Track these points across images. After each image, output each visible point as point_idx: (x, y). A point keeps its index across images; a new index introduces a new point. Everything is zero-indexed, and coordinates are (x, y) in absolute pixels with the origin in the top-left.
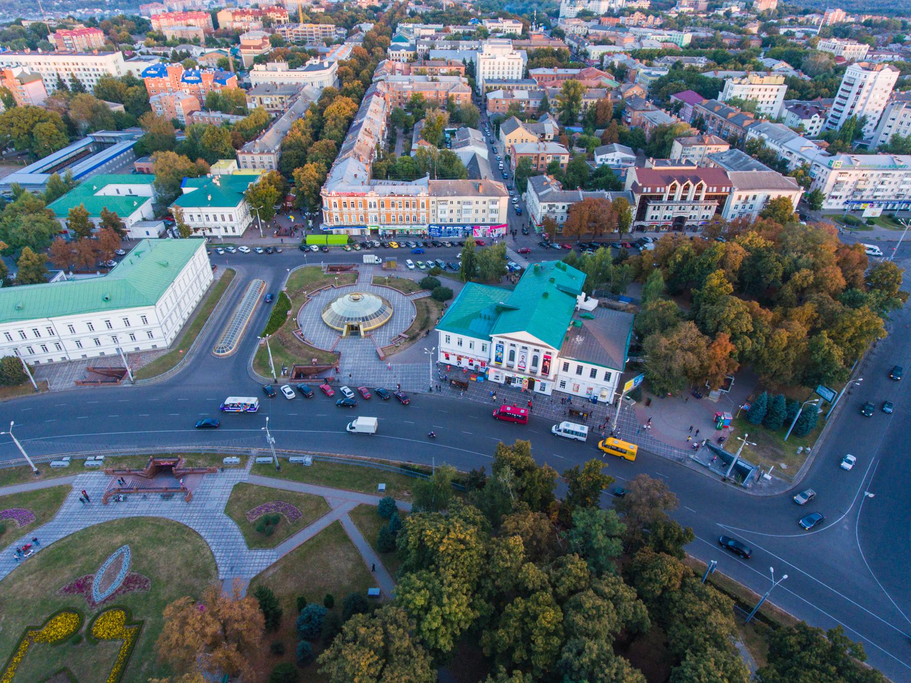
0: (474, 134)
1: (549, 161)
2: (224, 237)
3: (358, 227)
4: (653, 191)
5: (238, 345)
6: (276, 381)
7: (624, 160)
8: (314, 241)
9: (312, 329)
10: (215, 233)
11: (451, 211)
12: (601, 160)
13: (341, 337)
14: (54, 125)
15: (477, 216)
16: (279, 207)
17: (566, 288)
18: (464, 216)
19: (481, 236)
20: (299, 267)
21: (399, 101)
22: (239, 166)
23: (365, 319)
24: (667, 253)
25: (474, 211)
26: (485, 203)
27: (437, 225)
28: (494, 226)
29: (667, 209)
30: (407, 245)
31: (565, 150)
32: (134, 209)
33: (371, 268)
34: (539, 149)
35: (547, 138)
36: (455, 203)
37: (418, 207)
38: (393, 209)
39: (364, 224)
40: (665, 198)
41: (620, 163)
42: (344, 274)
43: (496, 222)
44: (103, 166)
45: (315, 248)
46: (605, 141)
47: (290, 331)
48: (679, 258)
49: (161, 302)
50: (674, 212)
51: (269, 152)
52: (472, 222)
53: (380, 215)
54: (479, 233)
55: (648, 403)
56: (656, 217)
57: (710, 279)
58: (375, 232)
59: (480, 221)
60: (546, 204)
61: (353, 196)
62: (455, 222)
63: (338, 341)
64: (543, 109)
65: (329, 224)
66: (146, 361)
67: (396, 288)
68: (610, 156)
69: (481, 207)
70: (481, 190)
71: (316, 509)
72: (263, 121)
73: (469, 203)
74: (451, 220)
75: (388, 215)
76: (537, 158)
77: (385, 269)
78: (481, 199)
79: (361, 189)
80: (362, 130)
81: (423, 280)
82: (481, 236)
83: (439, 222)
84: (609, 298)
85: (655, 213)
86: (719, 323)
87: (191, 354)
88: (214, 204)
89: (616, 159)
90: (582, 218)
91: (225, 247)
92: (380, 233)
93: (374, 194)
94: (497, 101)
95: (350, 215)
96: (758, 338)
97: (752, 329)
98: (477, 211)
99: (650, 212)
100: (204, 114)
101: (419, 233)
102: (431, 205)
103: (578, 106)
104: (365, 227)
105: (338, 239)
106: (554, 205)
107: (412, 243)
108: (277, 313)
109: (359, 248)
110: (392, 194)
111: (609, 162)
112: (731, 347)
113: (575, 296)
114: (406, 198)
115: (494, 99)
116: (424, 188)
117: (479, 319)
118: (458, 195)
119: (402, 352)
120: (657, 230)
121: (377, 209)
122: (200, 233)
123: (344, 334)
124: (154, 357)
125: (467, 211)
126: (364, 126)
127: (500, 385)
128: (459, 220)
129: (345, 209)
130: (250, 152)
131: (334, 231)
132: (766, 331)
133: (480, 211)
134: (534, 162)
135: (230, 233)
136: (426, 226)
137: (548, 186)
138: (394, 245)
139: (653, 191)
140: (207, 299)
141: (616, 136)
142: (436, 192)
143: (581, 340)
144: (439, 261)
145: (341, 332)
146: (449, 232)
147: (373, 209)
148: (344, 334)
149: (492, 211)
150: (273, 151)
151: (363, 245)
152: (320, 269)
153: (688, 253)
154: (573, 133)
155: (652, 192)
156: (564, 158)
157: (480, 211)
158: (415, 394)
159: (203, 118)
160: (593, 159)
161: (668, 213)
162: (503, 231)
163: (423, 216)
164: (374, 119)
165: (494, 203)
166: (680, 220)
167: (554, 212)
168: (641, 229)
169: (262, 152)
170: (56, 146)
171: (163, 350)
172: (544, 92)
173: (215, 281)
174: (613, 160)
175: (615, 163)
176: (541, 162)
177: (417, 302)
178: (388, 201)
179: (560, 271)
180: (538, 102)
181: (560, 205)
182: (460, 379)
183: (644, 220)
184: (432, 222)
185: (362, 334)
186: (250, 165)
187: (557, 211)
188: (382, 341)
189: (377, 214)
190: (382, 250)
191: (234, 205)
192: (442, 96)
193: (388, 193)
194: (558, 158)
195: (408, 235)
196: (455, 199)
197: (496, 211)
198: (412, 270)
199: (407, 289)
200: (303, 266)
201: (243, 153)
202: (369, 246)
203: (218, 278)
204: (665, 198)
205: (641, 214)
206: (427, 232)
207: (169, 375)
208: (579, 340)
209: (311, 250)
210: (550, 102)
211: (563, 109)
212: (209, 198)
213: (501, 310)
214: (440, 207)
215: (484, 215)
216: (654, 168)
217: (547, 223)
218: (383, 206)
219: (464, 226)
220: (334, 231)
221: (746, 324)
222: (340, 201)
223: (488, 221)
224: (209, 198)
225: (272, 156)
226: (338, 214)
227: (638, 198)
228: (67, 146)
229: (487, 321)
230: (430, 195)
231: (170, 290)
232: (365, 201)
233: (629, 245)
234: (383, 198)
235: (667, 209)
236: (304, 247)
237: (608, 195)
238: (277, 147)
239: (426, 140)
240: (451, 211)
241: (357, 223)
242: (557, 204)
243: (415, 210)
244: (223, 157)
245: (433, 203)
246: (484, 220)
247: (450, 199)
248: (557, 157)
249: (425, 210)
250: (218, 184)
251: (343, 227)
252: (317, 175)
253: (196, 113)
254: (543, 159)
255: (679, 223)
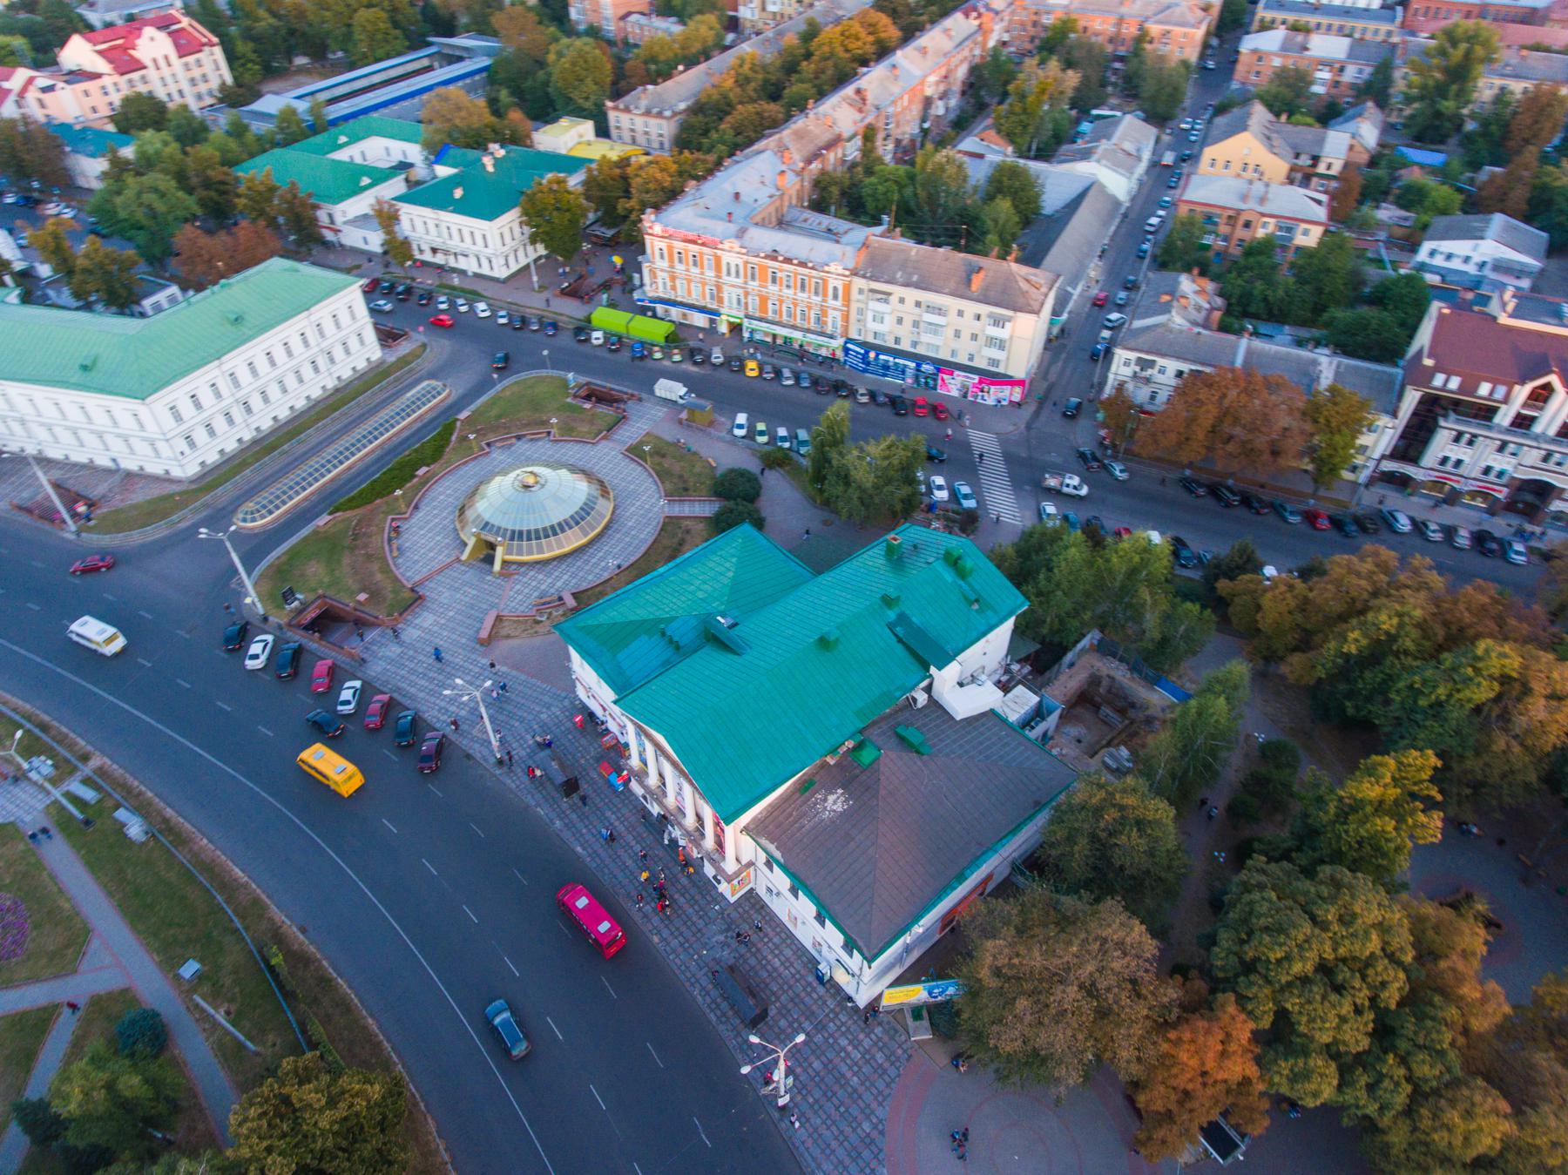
0: (1133, 133)
1: (1261, 233)
2: (476, 275)
3: (702, 310)
4: (1469, 387)
5: (286, 512)
6: (265, 619)
7: (1500, 266)
8: (607, 319)
9: (427, 522)
10: (462, 264)
11: (900, 321)
12: (1432, 253)
13: (458, 560)
14: (384, 15)
15: (955, 345)
16: (609, 233)
17: (920, 633)
18: (926, 338)
19: (955, 393)
20: (534, 373)
21: (1032, 31)
22: (603, 131)
23: (516, 535)
24: (1337, 607)
25: (950, 333)
26: (978, 318)
27: (863, 344)
28: (991, 378)
29: (1501, 449)
30: (778, 373)
31: (1321, 213)
32: (358, 190)
33: (660, 412)
34: (1244, 198)
35: (1321, 169)
36: (910, 302)
37: (825, 295)
38: (773, 289)
39: (714, 307)
40: (1504, 417)
41: (1487, 272)
42: (602, 409)
43: (1001, 370)
44: (416, 100)
45: (597, 337)
46: (1477, 205)
47: (388, 513)
48: (1355, 640)
49: (178, 393)
50: (1524, 463)
51: (660, 115)
52: (944, 355)
53: (747, 294)
54: (953, 386)
55: (956, 1059)
56: (1459, 463)
57: (1371, 772)
58: (736, 328)
59: (962, 359)
60: (1133, 355)
61: (694, 242)
62: (905, 346)
63: (448, 566)
64: (1375, 90)
65: (650, 291)
66: (139, 496)
67: (662, 475)
68: (1460, 247)
69: (968, 325)
70: (974, 287)
71: (52, 956)
72: (696, 47)
73: (940, 311)
74: (897, 340)
75: (764, 300)
76: (1232, 220)
77: (680, 422)
78: (972, 308)
79: (721, 227)
80: (849, 91)
81: (732, 471)
82: (955, 393)
83: (870, 339)
84: (1134, 668)
85: (1456, 452)
86: (1249, 967)
87: (206, 506)
88: (461, 208)
89: (1477, 258)
90: (1193, 420)
91: (454, 293)
92: (746, 335)
93: (736, 245)
94: (1259, 55)
95: (689, 281)
96: (1381, 1077)
97: (1357, 1038)
98: (957, 334)
99: (1442, 445)
100: (643, 20)
101: (824, 352)
102: (855, 295)
103: (1463, 96)
104: (716, 313)
105: (651, 330)
106: (1152, 364)
107: (786, 373)
108: (401, 466)
109: (677, 358)
110: (773, 255)
111: (1456, 264)
112: (1239, 1067)
113: (925, 666)
114: (800, 270)
115: (1254, 51)
116: (850, 251)
117: (657, 638)
118: (917, 286)
119: (537, 641)
120: (1453, 498)
121: (740, 281)
122: (439, 259)
123: (464, 557)
124: (156, 491)
125: (935, 328)
126: (862, 83)
127: (646, 814)
128: (915, 344)
129: (680, 268)
130: (627, 110)
131: (660, 308)
132: (1426, 1069)
133: (966, 335)
134: (1224, 229)
135: (486, 271)
136: (837, 343)
137: (1166, 309)
138: (752, 368)
139: (1469, 387)
140: (339, 396)
141: (1520, 194)
142: (874, 268)
143: (839, 807)
144: (803, 434)
145: (465, 545)
146: (886, 367)
147: (732, 279)
148: (464, 557)
149: (992, 342)
150: (668, 113)
151: (691, 354)
152: (565, 383)
153: (1392, 638)
154: (1405, 164)
155: (1461, 390)
156: (1306, 233)
157: (966, 335)
158: (468, 756)
159: (641, 27)
160: (1413, 248)
161: (1502, 463)
162: (1017, 394)
163: (833, 320)
164: (926, 68)
165: (998, 322)
166: (1543, 491)
167: (1148, 380)
168: (1401, 482)
169: (648, 113)
170: (380, 53)
171: (180, 481)
172: (1394, 46)
173: (381, 362)
174: (1467, 260)
175: (1471, 269)
176: (1241, 233)
177: (670, 524)
178: (763, 268)
179: (948, 576)
180: (1368, 70)
181: (1172, 366)
182: (582, 763)
183: (1414, 460)
184: (854, 335)
185: (497, 566)
186: (627, 136)
187: (1160, 378)
188: (519, 596)
189: (740, 291)
190: (724, 375)
191: (490, 214)
192: (1130, 30)
193: (768, 249)
194: (1289, 230)
195: (802, 354)
196: (912, 295)
197: (1001, 345)
198: (730, 443)
199: (679, 489)
200: (544, 373)
201: (616, 108)
202: (699, 358)
203: (392, 359)
204: (1504, 417)
205: (1413, 442)
206: (840, 355)
207: (136, 538)
208: (835, 802)
209: (588, 340)
210: (1397, 74)
211: (1422, 98)
212: (458, 193)
213: (715, 639)
214: (875, 306)
215: (972, 347)
216: (1504, 319)
217: (1120, 403)
218: (753, 278)
219: (919, 359)
220: (660, 308)
221: (1338, 1023)
222: (670, 248)
223: (981, 363)
224: (458, 193)
225: (664, 123)
226: (665, 275)
227: (1412, 398)
228: (400, 54)
229: (669, 652)
230: (854, 273)
231: (211, 372)
232: (718, 260)
233: (1324, 523)
234: (756, 260)
235: (1501, 449)
236: (583, 329)
237: (1327, 366)
238: (682, 106)
239: (999, 132)
240: (900, 321)
241: (702, 303)
242: (1161, 361)
243: (817, 299)
244: (581, 113)
245: (861, 291)
246: (971, 359)
247: (898, 291)
248: (1289, 224)
249: (838, 304)
250: (490, 169)
251: (674, 303)
252: (667, 181)
253: (634, 18)
254: (1247, 225)
255: (1532, 497)
